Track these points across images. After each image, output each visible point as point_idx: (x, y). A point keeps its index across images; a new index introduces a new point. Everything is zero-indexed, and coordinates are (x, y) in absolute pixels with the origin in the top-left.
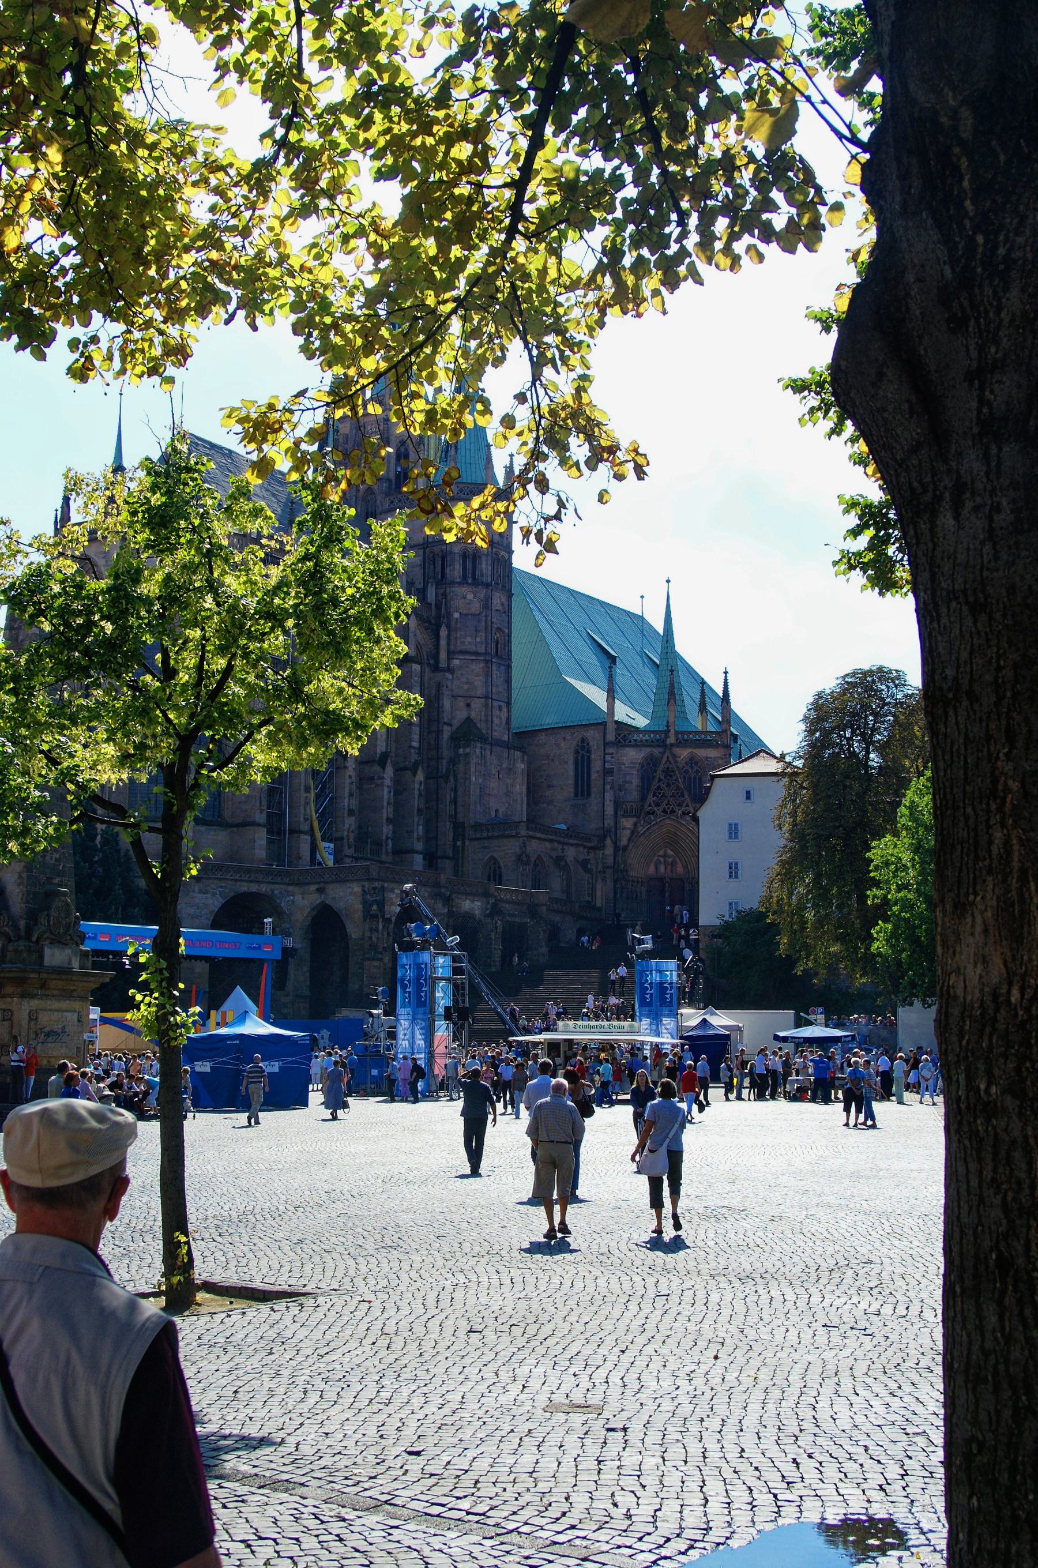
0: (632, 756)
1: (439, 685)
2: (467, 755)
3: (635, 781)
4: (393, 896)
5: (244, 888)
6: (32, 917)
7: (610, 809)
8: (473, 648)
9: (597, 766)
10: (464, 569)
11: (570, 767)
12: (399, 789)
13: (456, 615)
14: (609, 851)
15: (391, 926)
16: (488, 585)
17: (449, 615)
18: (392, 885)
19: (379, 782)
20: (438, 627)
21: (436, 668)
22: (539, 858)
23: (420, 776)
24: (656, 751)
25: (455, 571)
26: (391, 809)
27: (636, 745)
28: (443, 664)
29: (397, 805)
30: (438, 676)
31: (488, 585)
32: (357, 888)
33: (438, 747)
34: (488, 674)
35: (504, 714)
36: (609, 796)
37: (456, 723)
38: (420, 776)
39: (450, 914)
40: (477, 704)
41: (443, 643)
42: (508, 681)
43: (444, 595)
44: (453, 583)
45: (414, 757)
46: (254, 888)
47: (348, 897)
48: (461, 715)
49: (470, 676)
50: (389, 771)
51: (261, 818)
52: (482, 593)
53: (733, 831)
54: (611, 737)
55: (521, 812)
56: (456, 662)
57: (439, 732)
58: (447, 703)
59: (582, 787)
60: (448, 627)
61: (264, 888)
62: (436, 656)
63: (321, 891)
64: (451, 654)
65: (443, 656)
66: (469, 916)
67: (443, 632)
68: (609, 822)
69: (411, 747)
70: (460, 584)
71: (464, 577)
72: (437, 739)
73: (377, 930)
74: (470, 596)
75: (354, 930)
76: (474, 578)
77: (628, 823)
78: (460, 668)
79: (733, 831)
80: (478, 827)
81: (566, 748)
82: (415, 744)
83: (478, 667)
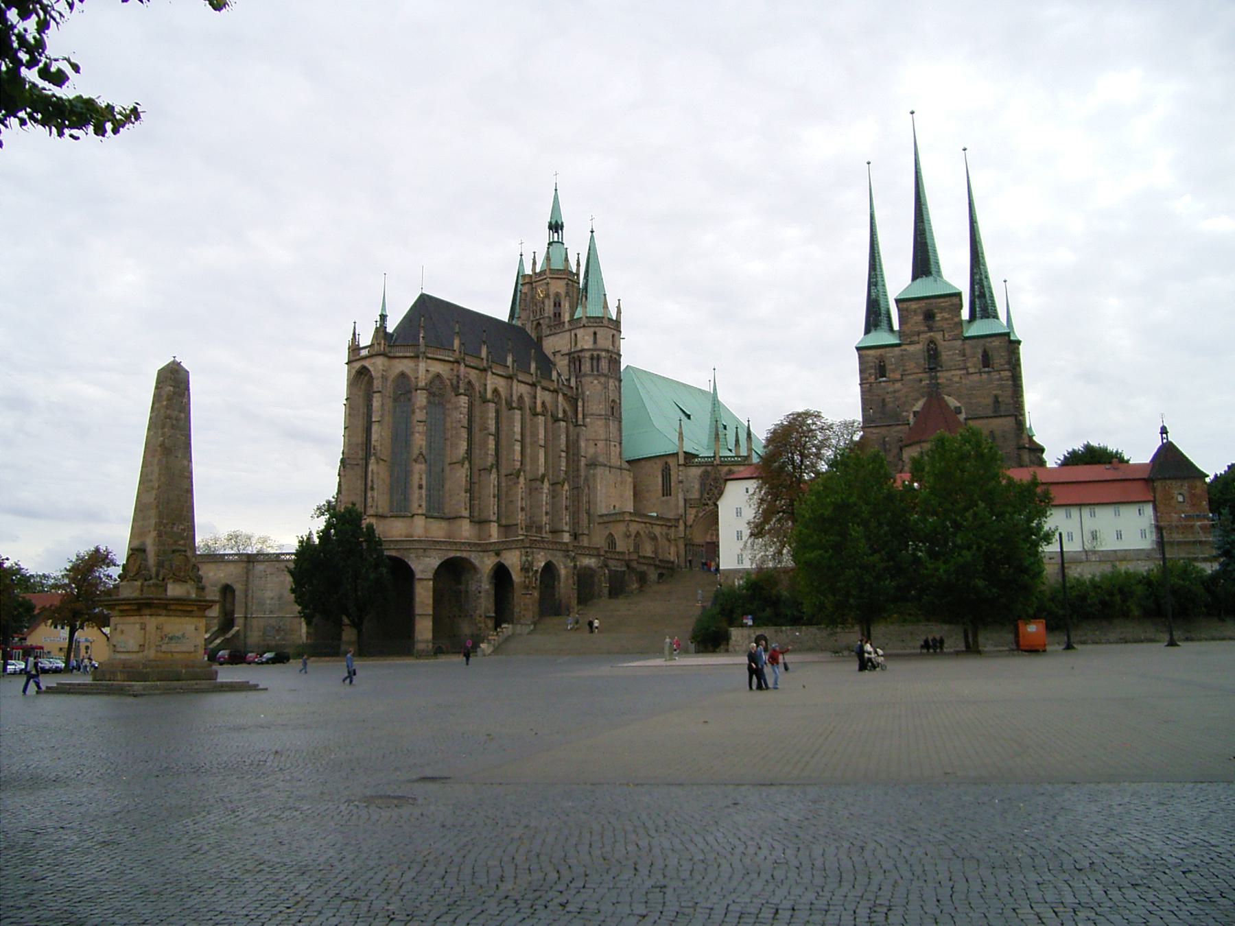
0: (695, 472)
1: (578, 435)
2: (594, 475)
3: (697, 486)
5: (452, 554)
6: (160, 565)
7: (681, 503)
8: (598, 412)
9: (674, 478)
11: (660, 480)
12: (554, 495)
14: (682, 528)
16: (605, 376)
17: (583, 393)
20: (577, 400)
21: (577, 425)
22: (638, 533)
24: (709, 468)
25: (586, 367)
27: (699, 465)
28: (580, 422)
29: (553, 505)
31: (605, 376)
32: (517, 553)
34: (607, 426)
35: (618, 450)
36: (681, 496)
38: (566, 487)
39: (575, 566)
40: (601, 444)
41: (580, 409)
42: (620, 430)
44: (585, 375)
45: (563, 475)
46: (458, 554)
47: (513, 560)
48: (591, 450)
49: (595, 428)
50: (546, 485)
51: (466, 513)
52: (603, 380)
54: (681, 461)
55: (630, 507)
57: (579, 461)
58: (583, 444)
59: (667, 491)
61: (465, 555)
63: (498, 554)
65: (580, 416)
66: (589, 568)
67: (580, 404)
68: (681, 511)
75: (517, 577)
77: (692, 513)
80: (601, 516)
81: (657, 469)
82: (563, 468)
83: (601, 423)
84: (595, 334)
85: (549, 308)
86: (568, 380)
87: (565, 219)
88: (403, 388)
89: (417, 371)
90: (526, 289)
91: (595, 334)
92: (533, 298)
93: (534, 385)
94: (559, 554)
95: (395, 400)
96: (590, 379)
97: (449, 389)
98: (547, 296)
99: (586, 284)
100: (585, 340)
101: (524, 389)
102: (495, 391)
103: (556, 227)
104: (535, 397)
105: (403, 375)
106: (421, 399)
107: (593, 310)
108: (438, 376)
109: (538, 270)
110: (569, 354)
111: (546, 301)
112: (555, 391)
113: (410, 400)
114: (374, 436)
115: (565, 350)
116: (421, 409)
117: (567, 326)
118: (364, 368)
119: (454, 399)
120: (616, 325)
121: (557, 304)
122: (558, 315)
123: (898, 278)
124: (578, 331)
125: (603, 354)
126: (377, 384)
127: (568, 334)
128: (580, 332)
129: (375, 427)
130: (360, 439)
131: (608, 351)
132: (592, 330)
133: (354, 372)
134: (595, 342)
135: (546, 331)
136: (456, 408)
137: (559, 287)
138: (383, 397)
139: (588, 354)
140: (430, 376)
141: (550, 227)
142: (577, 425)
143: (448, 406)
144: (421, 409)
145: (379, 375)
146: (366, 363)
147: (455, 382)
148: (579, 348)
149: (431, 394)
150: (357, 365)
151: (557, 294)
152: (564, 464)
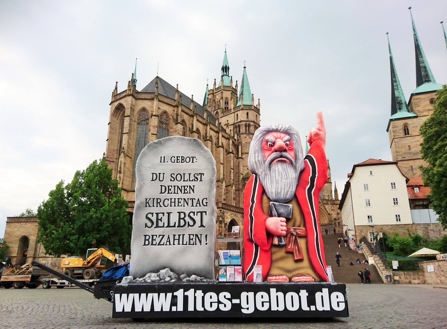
1: (239, 163)
4: (227, 215)
10: (246, 130)
13: (244, 142)
15: (227, 227)
17: (241, 143)
18: (227, 211)
19: (221, 187)
23: (234, 188)
25: (243, 130)
26: (225, 196)
28: (240, 156)
30: (239, 160)
33: (239, 181)
37: (244, 174)
38: (234, 188)
41: (240, 150)
43: (240, 137)
44: (242, 134)
50: (224, 184)
53: (366, 187)
56: (244, 156)
57: (239, 176)
58: (241, 168)
60: (241, 146)
62: (238, 154)
64: (242, 154)
67: (240, 147)
69: (231, 179)
70: (245, 134)
71: (246, 131)
72: (239, 179)
73: (221, 227)
74: (248, 137)
76: (249, 132)
78: (245, 157)
79: (366, 187)
82: (232, 178)
84: (247, 114)
85: (223, 105)
86: (234, 136)
87: (230, 65)
88: (144, 117)
89: (152, 107)
90: (210, 97)
91: (247, 114)
92: (214, 100)
93: (218, 132)
94: (239, 215)
95: (138, 124)
96: (245, 135)
97: (171, 121)
98: (222, 98)
99: (242, 94)
100: (242, 116)
101: (213, 134)
102: (198, 129)
103: (225, 69)
104: (218, 138)
105: (144, 109)
106: (154, 122)
107: (247, 101)
108: (165, 112)
109: (217, 87)
110: (233, 124)
111: (221, 101)
112: (228, 139)
113: (147, 124)
114: (125, 142)
115: (231, 122)
116: (154, 127)
117: (232, 111)
118: (121, 105)
119: (175, 127)
120: (257, 110)
121: (227, 103)
122: (227, 108)
123: (408, 86)
124: (238, 113)
125: (252, 123)
126: (128, 112)
127: (233, 114)
128: (240, 113)
129: (125, 137)
130: (115, 147)
131: (254, 122)
132: (246, 111)
133: (114, 108)
134: (248, 117)
135: (220, 115)
136: (176, 131)
137: (227, 94)
138: (131, 120)
139: (244, 123)
140: (160, 111)
141: (223, 69)
142: (238, 158)
143: (171, 130)
144: (154, 127)
145: (129, 107)
146: (121, 101)
147: (175, 117)
148: (239, 120)
149: (161, 122)
150: (116, 104)
151: (227, 98)
152: (232, 176)
